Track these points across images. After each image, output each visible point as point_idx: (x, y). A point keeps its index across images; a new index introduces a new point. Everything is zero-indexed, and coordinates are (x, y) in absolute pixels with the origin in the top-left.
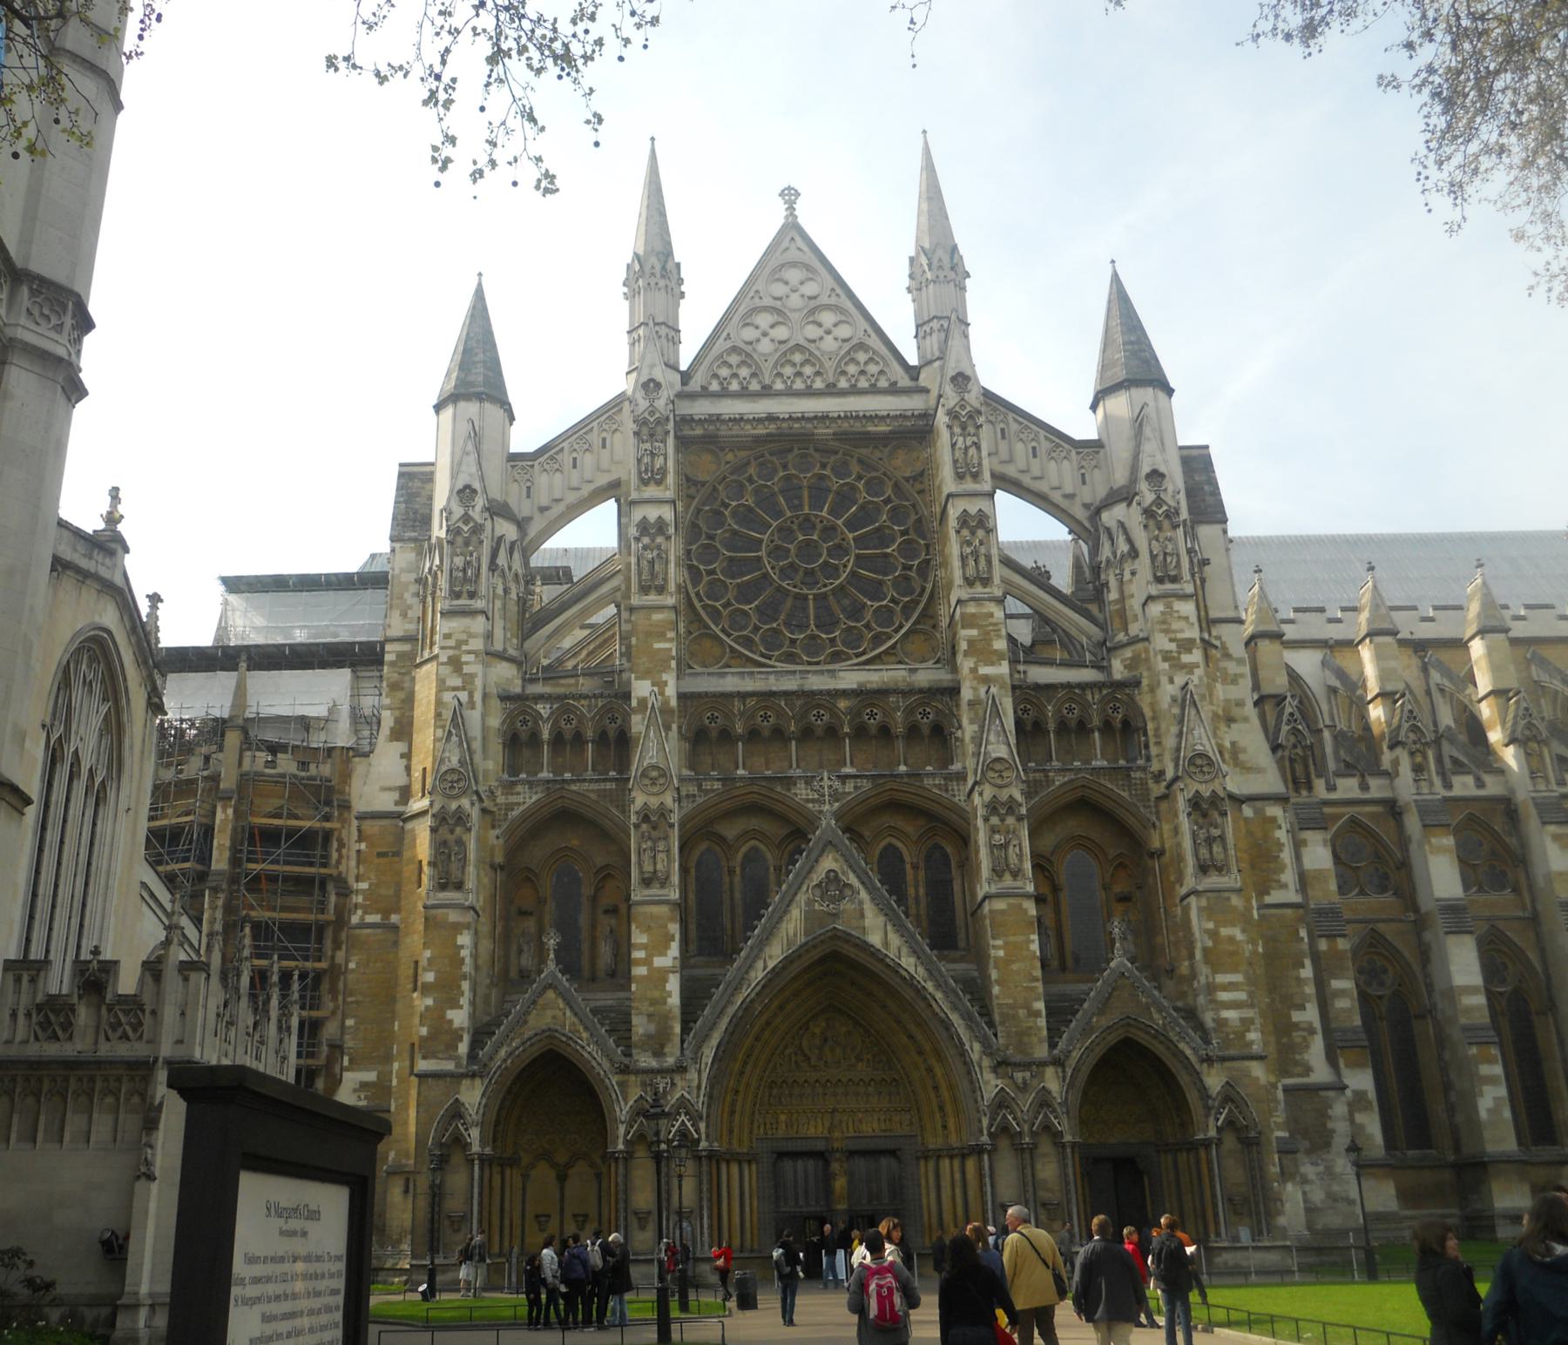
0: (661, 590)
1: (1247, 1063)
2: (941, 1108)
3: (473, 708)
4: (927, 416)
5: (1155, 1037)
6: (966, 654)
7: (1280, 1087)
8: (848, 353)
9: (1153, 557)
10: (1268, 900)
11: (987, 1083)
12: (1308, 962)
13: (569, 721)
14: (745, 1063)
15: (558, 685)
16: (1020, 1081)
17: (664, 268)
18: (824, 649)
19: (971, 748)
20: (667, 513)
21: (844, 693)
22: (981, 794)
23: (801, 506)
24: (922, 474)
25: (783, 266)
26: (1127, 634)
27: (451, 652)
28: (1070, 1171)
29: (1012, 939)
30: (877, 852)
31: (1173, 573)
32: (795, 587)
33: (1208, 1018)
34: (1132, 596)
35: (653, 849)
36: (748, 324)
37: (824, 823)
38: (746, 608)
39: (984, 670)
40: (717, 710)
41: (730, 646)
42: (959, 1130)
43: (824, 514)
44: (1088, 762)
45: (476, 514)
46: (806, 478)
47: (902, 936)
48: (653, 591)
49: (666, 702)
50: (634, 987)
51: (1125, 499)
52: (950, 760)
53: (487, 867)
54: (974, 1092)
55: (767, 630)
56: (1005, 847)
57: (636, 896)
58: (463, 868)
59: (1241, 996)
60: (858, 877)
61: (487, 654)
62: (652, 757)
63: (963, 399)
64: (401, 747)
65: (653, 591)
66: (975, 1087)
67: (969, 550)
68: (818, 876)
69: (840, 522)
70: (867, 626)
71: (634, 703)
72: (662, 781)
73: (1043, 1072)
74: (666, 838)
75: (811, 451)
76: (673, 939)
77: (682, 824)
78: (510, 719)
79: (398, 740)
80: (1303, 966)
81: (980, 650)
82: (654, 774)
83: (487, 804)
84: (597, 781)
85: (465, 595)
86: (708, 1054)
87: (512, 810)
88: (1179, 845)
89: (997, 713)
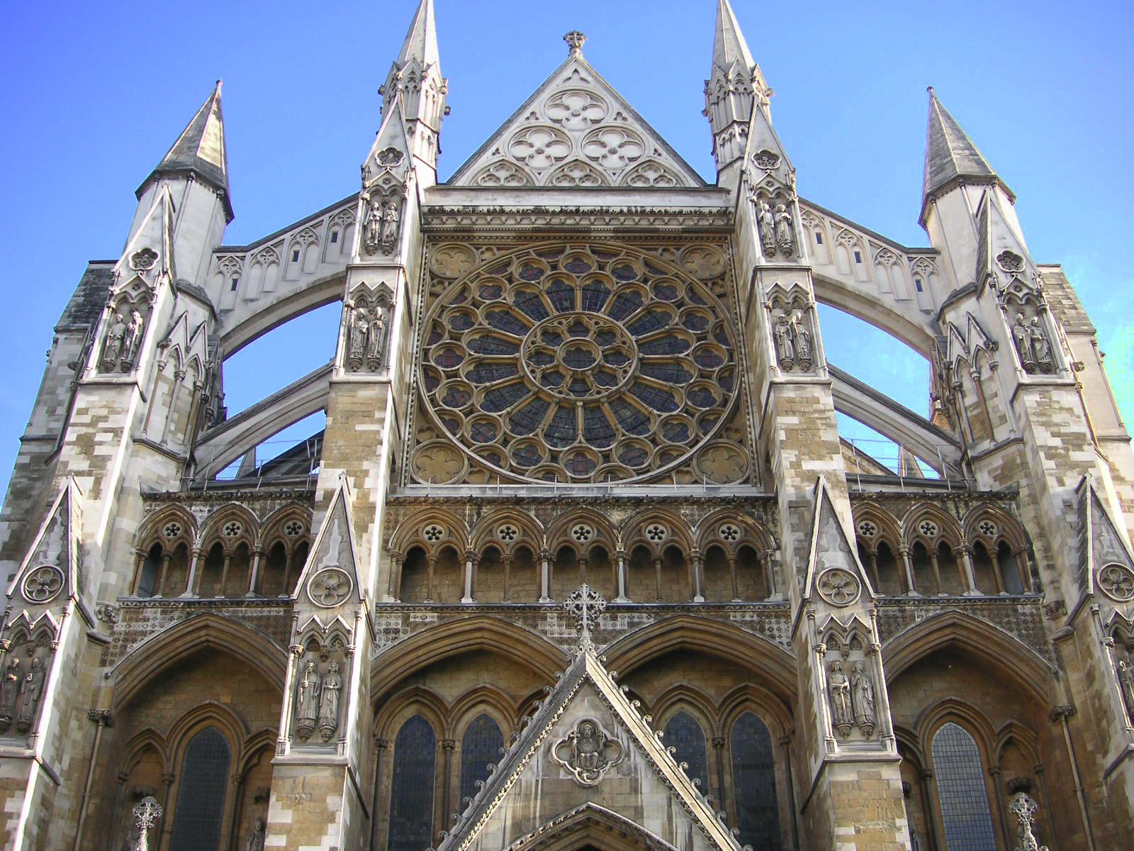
4: (724, 213)
8: (636, 169)
9: (1018, 343)
18: (595, 466)
21: (618, 502)
22: (811, 616)
23: (573, 308)
24: (722, 277)
25: (564, 92)
26: (993, 439)
27: (84, 430)
31: (1045, 361)
32: (560, 392)
34: (996, 395)
36: (520, 143)
39: (808, 465)
41: (470, 458)
43: (599, 314)
46: (578, 282)
49: (364, 496)
51: (975, 291)
55: (521, 442)
57: (287, 750)
65: (364, 368)
67: (783, 329)
69: (620, 324)
70: (654, 441)
71: (319, 496)
74: (340, 671)
75: (588, 251)
77: (375, 670)
78: (153, 524)
81: (807, 442)
82: (333, 582)
83: (99, 630)
85: (118, 368)
87: (134, 641)
88: (1098, 695)
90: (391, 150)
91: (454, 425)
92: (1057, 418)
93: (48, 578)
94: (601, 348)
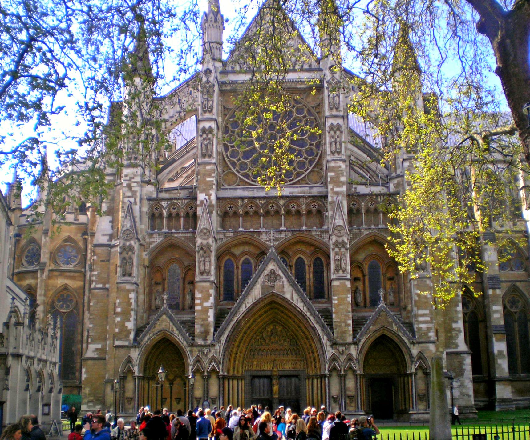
0: (210, 156)
1: (428, 345)
2: (314, 360)
5: (394, 334)
7: (445, 353)
11: (328, 351)
13: (174, 209)
14: (240, 342)
15: (170, 193)
16: (341, 351)
17: (216, 19)
19: (330, 220)
20: (213, 125)
24: (319, 105)
26: (396, 174)
27: (127, 182)
28: (358, 384)
30: (295, 260)
33: (415, 326)
35: (204, 261)
37: (270, 251)
38: (246, 161)
39: (336, 189)
40: (233, 204)
41: (240, 178)
42: (320, 368)
44: (378, 225)
47: (298, 295)
48: (207, 157)
49: (211, 202)
50: (196, 314)
52: (323, 225)
53: (142, 267)
54: (323, 354)
56: (339, 260)
58: (132, 268)
59: (428, 319)
60: (282, 272)
61: (142, 182)
62: (204, 225)
63: (333, 76)
64: (109, 218)
65: (207, 157)
66: (324, 353)
67: (332, 140)
68: (266, 272)
71: (198, 202)
72: (208, 234)
73: (350, 348)
74: (209, 257)
76: (211, 295)
77: (217, 250)
78: (151, 207)
79: (108, 215)
80: (458, 306)
82: (205, 231)
83: (142, 242)
84: (184, 233)
85: (133, 159)
86: (223, 339)
89: (339, 207)
90: (208, 69)
93: (128, 232)
94: (279, 135)
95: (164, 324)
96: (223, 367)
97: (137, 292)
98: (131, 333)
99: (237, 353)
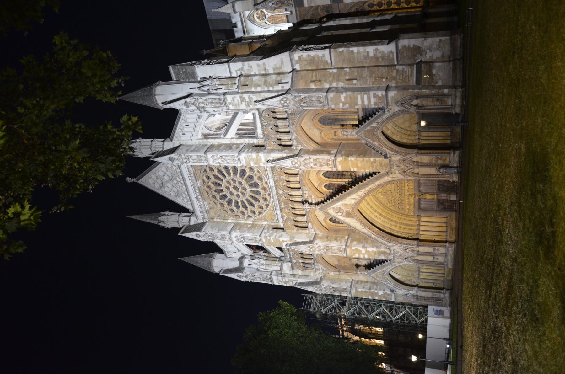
3: (297, 280)
6: (259, 165)
9: (214, 107)
10: (329, 61)
12: (351, 49)
14: (392, 221)
16: (397, 168)
20: (233, 235)
29: (350, 165)
31: (218, 100)
36: (170, 194)
39: (263, 160)
45: (245, 275)
49: (289, 241)
53: (340, 276)
59: (365, 96)
62: (305, 249)
76: (356, 249)
80: (352, 51)
86: (389, 244)
90: (196, 236)
91: (260, 213)
92: (237, 102)
95: (379, 275)
96: (410, 245)
97: (357, 283)
98: (386, 293)
99: (401, 223)
